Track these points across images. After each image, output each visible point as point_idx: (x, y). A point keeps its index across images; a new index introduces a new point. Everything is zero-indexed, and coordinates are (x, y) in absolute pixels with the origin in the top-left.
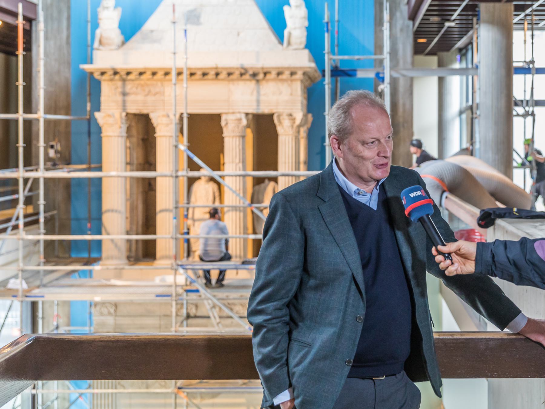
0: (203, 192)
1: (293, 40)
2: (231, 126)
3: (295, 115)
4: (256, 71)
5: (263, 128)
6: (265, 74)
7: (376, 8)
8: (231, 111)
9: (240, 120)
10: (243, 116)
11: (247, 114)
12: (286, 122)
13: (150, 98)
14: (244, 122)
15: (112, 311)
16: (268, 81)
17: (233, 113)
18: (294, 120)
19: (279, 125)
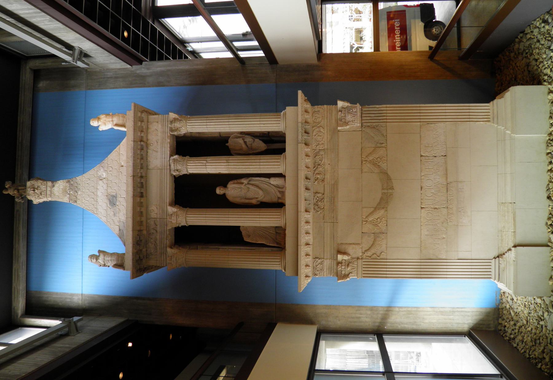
0: (233, 191)
1: (120, 122)
2: (179, 167)
3: (171, 119)
4: (139, 147)
5: (186, 146)
6: (141, 141)
7: (134, 87)
8: (168, 167)
9: (174, 159)
10: (172, 158)
11: (171, 155)
12: (177, 125)
13: (158, 230)
14: (176, 157)
15: (319, 261)
16: (147, 140)
17: (170, 165)
18: (175, 120)
19: (180, 131)
